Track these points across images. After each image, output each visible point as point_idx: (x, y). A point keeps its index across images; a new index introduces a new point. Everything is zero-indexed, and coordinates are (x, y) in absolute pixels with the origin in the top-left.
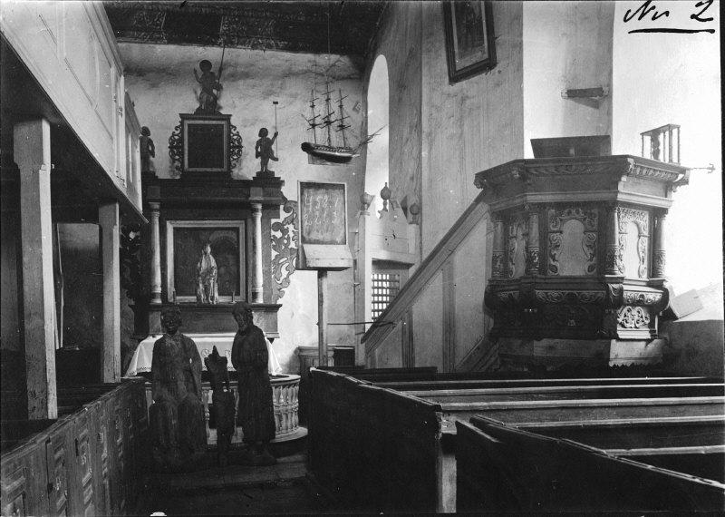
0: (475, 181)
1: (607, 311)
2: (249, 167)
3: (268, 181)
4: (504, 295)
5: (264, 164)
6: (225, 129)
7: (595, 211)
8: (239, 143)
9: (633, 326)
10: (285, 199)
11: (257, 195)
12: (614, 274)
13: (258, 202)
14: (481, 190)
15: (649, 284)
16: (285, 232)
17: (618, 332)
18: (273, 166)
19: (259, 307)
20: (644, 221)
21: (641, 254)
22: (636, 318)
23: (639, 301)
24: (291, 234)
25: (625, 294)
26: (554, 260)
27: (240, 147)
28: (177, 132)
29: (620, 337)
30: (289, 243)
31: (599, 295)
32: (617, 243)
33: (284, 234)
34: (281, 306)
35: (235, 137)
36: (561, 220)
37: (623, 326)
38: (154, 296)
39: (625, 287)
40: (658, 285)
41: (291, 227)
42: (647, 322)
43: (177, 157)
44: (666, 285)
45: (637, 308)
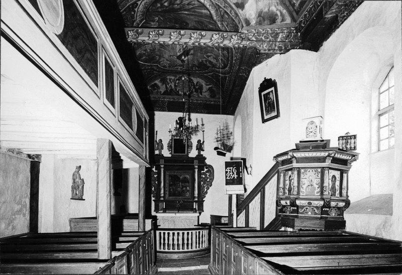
2: (193, 153)
3: (201, 159)
5: (199, 153)
18: (202, 153)
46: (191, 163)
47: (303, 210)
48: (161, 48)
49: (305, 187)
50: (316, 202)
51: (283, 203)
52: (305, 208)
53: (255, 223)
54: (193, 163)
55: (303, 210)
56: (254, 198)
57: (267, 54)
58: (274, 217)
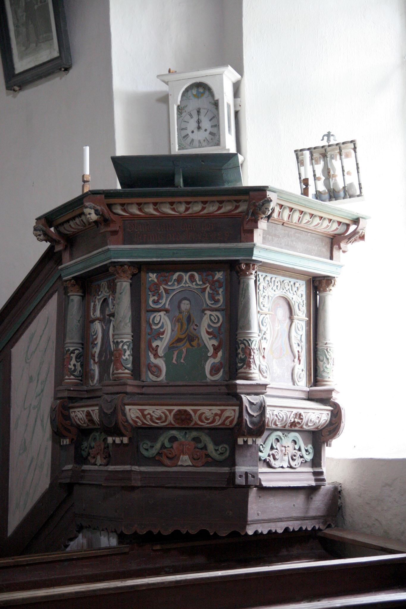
1: (240, 441)
4: (79, 414)
7: (219, 275)
9: (286, 465)
15: (310, 397)
17: (260, 476)
20: (299, 294)
21: (296, 349)
22: (291, 451)
23: (293, 424)
25: (268, 411)
26: (156, 356)
29: (265, 484)
31: (227, 414)
32: (254, 328)
37: (269, 466)
39: (269, 401)
40: (324, 399)
42: (309, 457)
44: (336, 398)
45: (293, 435)
47: (158, 446)
49: (162, 344)
50: (208, 411)
52: (164, 439)
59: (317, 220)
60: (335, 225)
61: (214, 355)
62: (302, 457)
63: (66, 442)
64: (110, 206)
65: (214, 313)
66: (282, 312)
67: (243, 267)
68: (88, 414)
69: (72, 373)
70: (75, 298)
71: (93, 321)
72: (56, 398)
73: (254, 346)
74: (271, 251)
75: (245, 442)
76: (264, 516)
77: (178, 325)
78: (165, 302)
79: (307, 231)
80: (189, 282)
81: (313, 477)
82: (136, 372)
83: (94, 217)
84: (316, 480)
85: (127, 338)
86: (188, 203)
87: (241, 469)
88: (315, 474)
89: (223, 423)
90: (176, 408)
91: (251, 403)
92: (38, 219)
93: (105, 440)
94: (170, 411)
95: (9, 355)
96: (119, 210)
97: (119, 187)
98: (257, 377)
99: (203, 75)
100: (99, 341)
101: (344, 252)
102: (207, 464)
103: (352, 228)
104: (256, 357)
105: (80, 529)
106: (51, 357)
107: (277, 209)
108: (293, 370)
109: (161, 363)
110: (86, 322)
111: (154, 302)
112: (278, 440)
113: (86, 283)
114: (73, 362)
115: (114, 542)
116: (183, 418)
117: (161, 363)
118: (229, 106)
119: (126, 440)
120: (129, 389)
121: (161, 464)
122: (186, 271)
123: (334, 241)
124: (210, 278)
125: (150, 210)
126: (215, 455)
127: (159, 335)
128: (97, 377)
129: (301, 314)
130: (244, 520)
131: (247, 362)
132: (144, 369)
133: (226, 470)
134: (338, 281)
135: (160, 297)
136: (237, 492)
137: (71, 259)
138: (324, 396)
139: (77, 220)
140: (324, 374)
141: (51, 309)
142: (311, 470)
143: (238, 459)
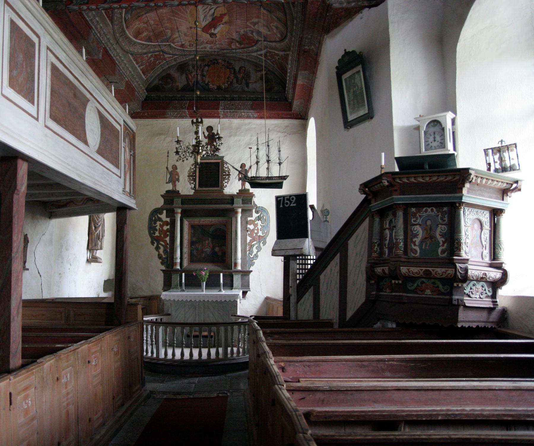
0: (359, 189)
1: (455, 285)
4: (379, 270)
5: (243, 185)
6: (220, 164)
7: (445, 209)
8: (229, 173)
9: (478, 297)
10: (256, 205)
11: (238, 202)
12: (460, 256)
13: (239, 207)
14: (364, 196)
15: (491, 266)
16: (256, 225)
17: (465, 301)
19: (238, 272)
20: (485, 217)
21: (484, 243)
22: (480, 290)
23: (482, 278)
24: (260, 227)
26: (415, 245)
27: (229, 175)
28: (193, 167)
29: (467, 305)
30: (258, 232)
31: (449, 272)
32: (463, 233)
33: (255, 227)
34: (251, 271)
35: (226, 169)
36: (420, 216)
37: (469, 296)
38: (176, 264)
39: (470, 267)
40: (499, 267)
41: (259, 223)
42: (490, 294)
43: (192, 182)
44: (505, 267)
45: (482, 283)
46: (228, 203)
47: (415, 285)
48: (174, 16)
49: (417, 240)
51: (379, 270)
52: (418, 282)
53: (330, 311)
54: (233, 203)
55: (415, 285)
56: (328, 263)
57: (346, 10)
58: (363, 299)
59: (495, 183)
60: (505, 185)
61: (443, 245)
62: (486, 293)
63: (373, 282)
64: (394, 179)
65: (443, 226)
66: (477, 226)
67: (457, 205)
68: (383, 270)
69: (375, 252)
70: (377, 219)
71: (386, 229)
72: (368, 263)
73: (463, 241)
74: (472, 197)
75: (458, 285)
76: (465, 319)
77: (425, 232)
78: (419, 221)
79: (490, 188)
80: (429, 211)
81: (492, 303)
82: (406, 252)
83: (386, 184)
84: (493, 305)
85: (402, 237)
86: (430, 176)
87: (455, 297)
88: (493, 302)
89: (447, 276)
90: (424, 269)
91: (461, 268)
92: (361, 185)
93: (391, 281)
94: (421, 270)
95: (347, 244)
96: (398, 181)
97: (397, 170)
98: (464, 256)
99: (437, 116)
100: (388, 238)
101: (510, 197)
102: (438, 295)
103: (514, 186)
104: (464, 247)
105: (379, 320)
106: (366, 245)
107: (475, 178)
108: (482, 253)
109: (417, 248)
110: (382, 230)
111: (414, 221)
112: (474, 285)
113: (382, 213)
114: (376, 247)
115: (394, 326)
116: (427, 273)
117: (417, 248)
118: (449, 130)
119: (400, 282)
120: (402, 260)
121: (417, 293)
122: (429, 207)
123: (504, 192)
124: (441, 210)
125: (413, 180)
126: (443, 290)
127: (416, 236)
128: (387, 254)
129: (487, 227)
130: (456, 321)
131: (459, 248)
132: (409, 251)
133: (448, 297)
134: (507, 212)
135: (417, 219)
136: (454, 308)
137: (376, 202)
138: (498, 265)
139: (378, 185)
140: (499, 255)
141: (366, 224)
142: (490, 300)
143: (454, 293)
